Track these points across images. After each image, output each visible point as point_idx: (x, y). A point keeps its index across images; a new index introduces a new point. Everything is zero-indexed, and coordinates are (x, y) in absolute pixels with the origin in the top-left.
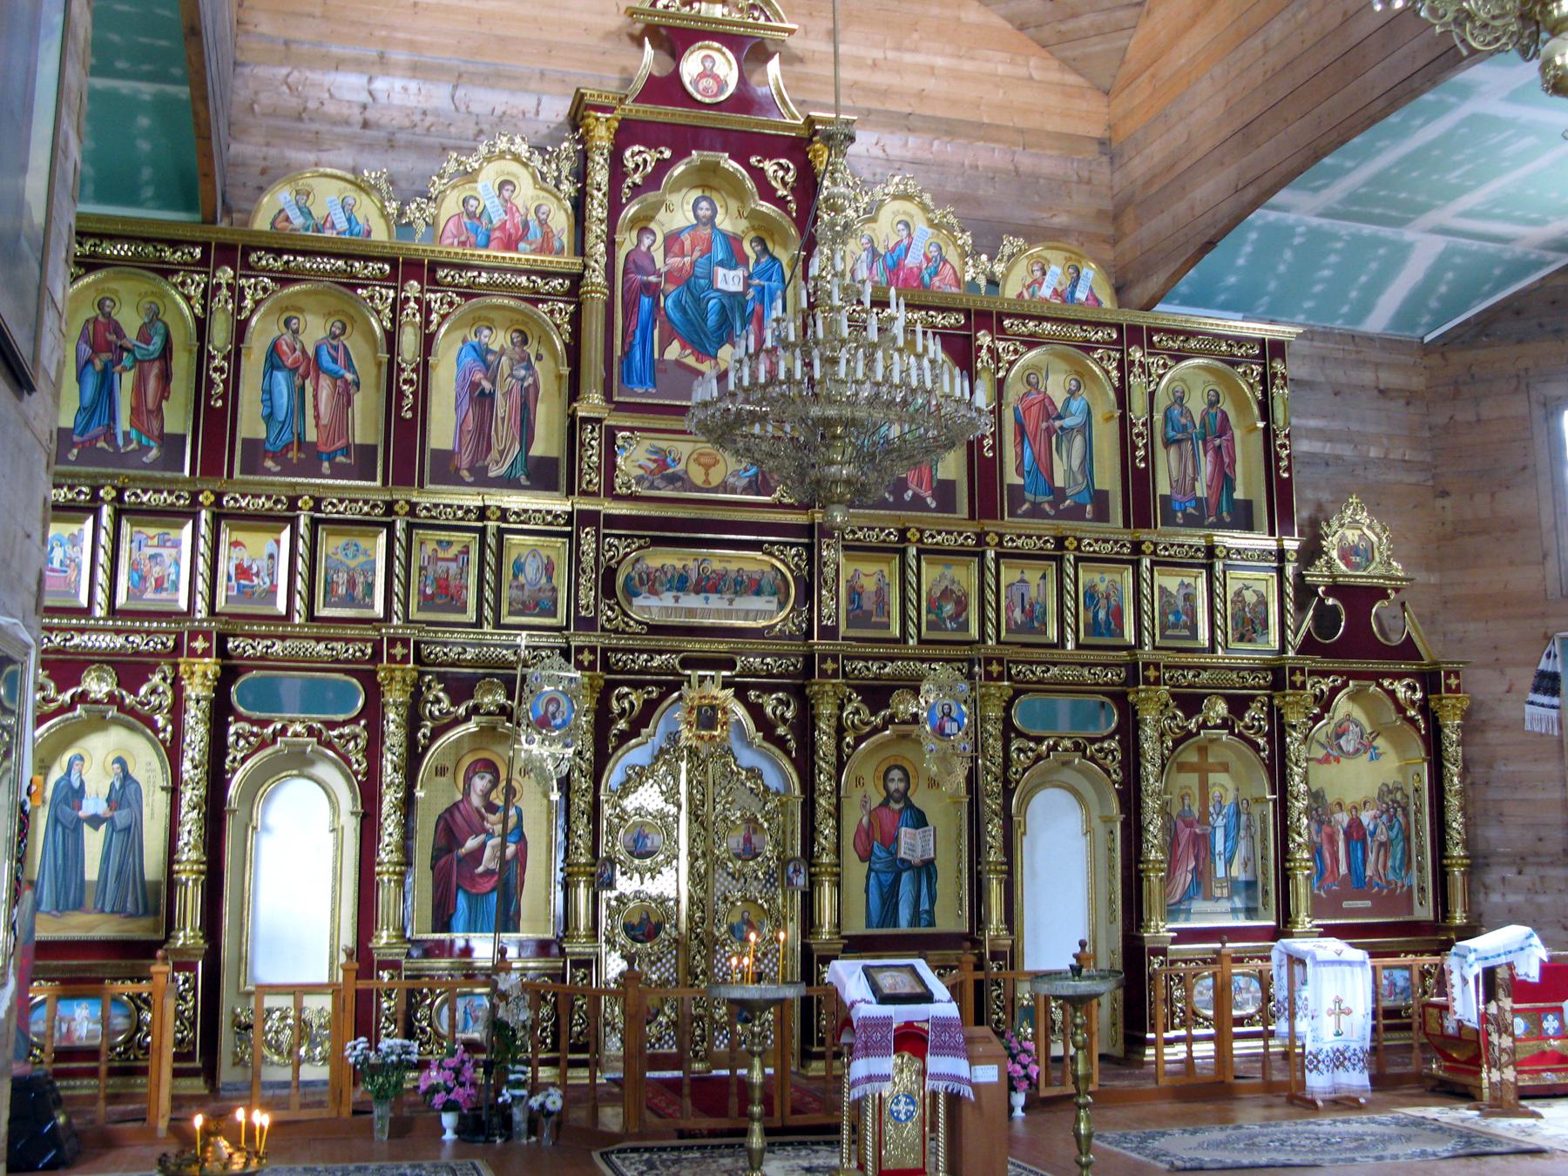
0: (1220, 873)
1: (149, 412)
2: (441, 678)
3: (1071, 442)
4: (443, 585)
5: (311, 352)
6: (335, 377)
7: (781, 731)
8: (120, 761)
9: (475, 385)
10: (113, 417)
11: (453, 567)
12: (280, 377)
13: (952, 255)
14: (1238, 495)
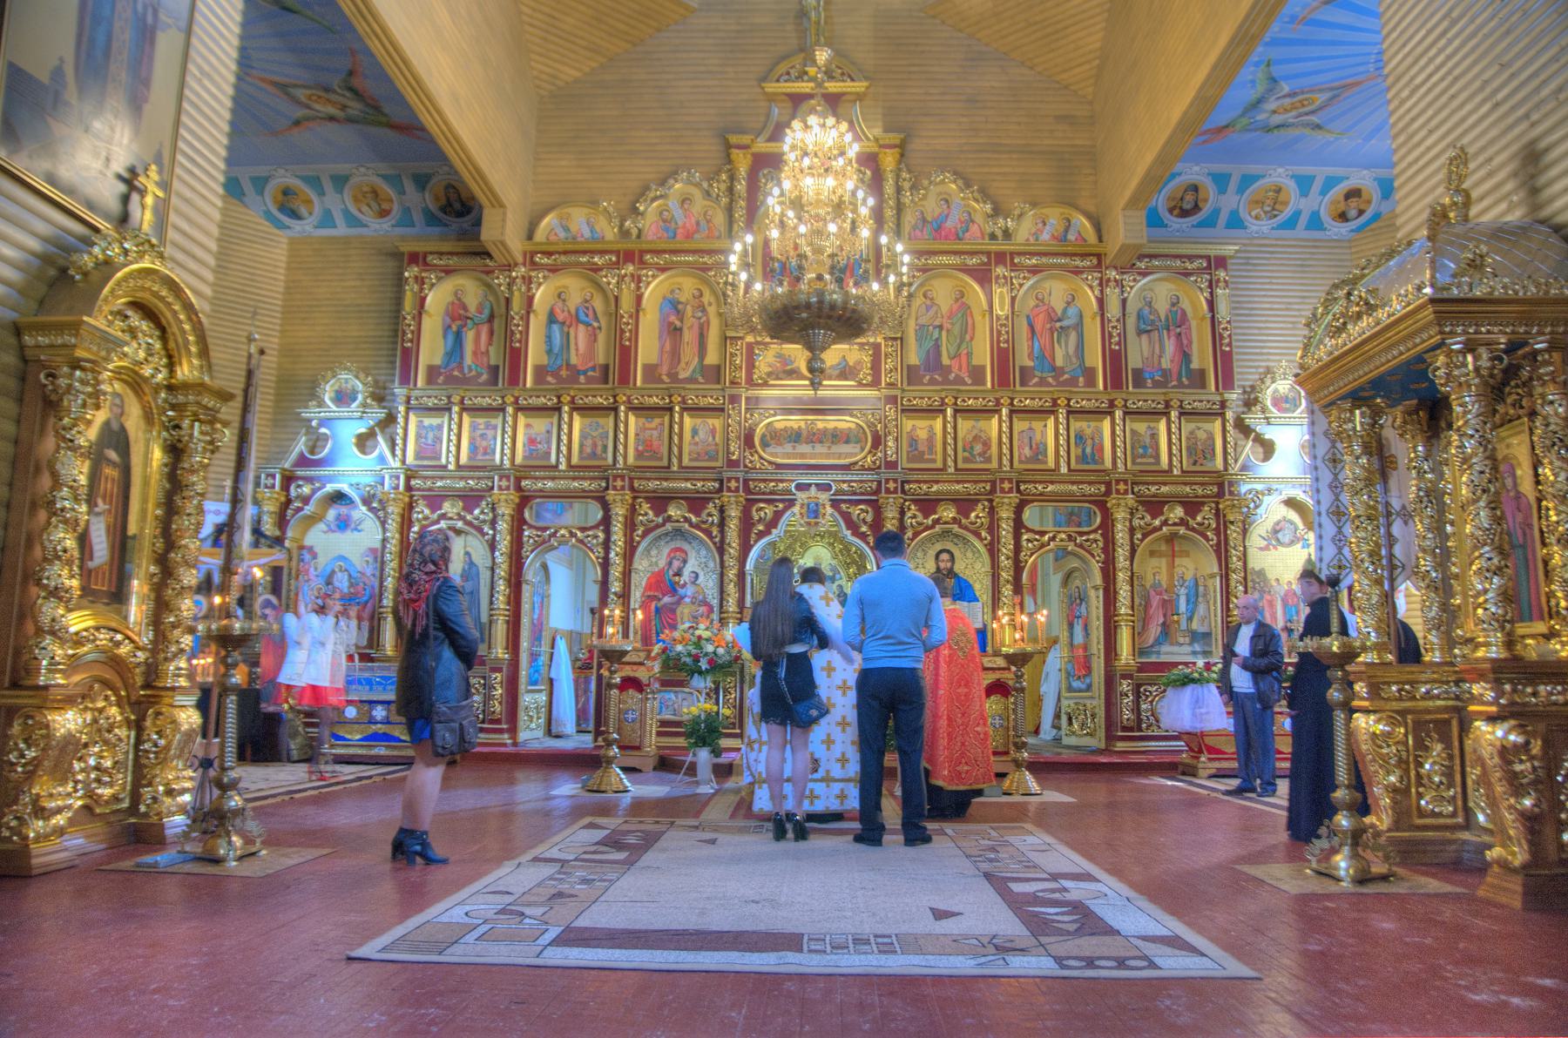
0: (1184, 626)
2: (648, 499)
4: (648, 445)
5: (573, 311)
6: (588, 325)
7: (864, 529)
8: (467, 553)
9: (671, 324)
10: (462, 357)
11: (655, 433)
12: (555, 327)
13: (979, 219)
14: (1195, 365)
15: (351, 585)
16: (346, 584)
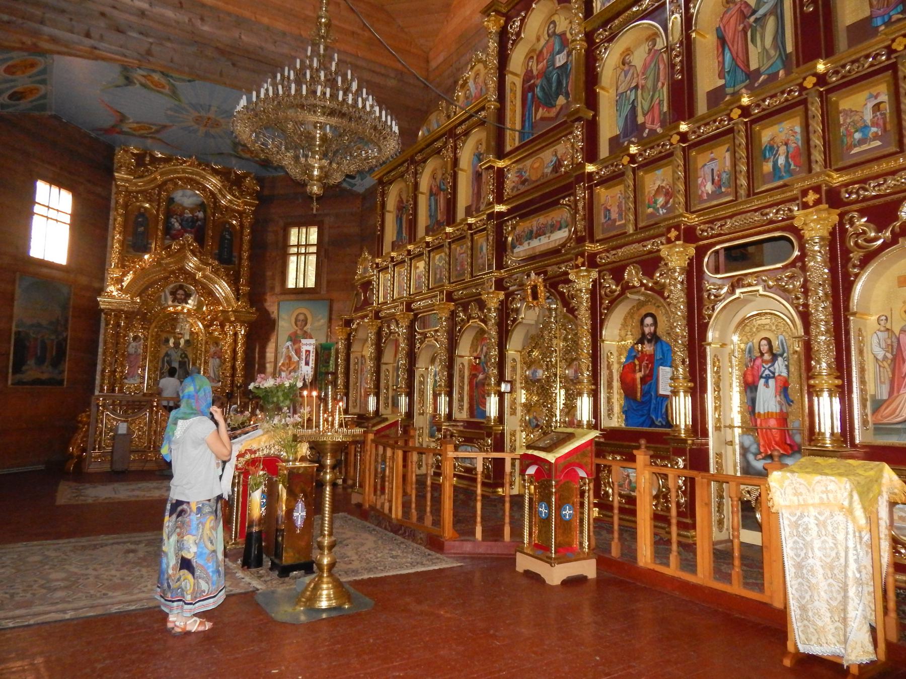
3: (763, 27)
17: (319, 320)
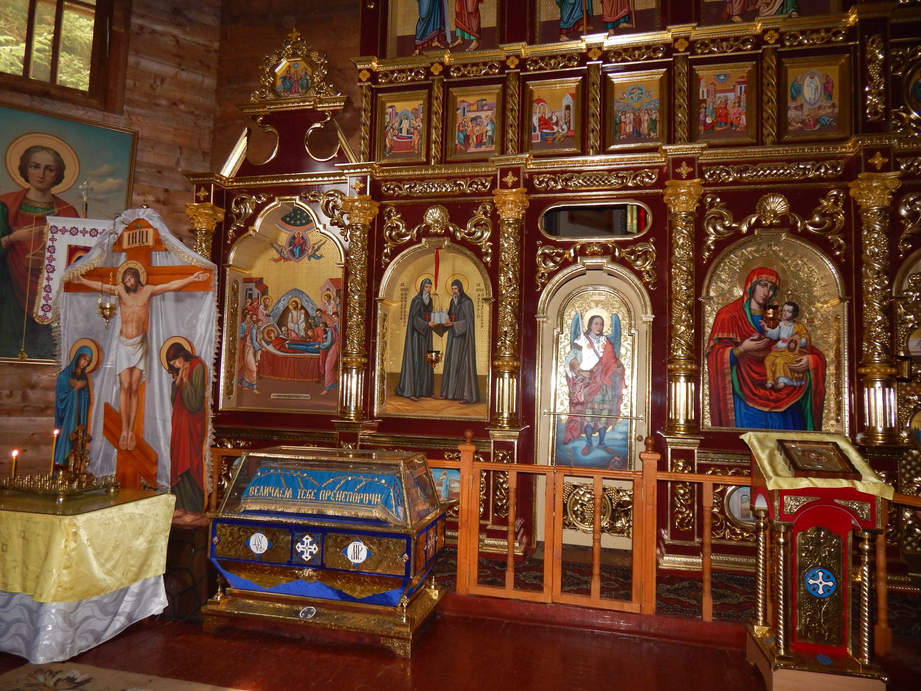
1: (470, 14)
8: (457, 283)
10: (443, 23)
15: (309, 326)
16: (303, 326)
17: (102, 177)
